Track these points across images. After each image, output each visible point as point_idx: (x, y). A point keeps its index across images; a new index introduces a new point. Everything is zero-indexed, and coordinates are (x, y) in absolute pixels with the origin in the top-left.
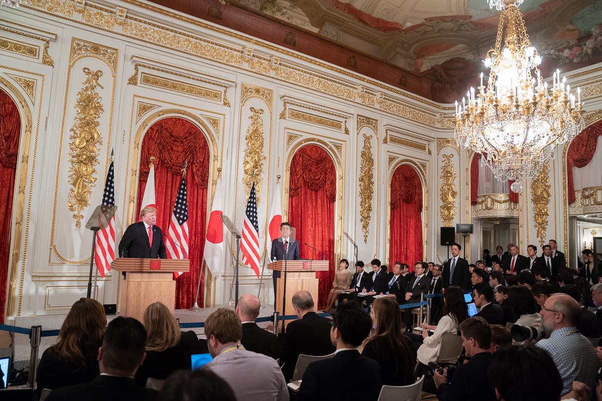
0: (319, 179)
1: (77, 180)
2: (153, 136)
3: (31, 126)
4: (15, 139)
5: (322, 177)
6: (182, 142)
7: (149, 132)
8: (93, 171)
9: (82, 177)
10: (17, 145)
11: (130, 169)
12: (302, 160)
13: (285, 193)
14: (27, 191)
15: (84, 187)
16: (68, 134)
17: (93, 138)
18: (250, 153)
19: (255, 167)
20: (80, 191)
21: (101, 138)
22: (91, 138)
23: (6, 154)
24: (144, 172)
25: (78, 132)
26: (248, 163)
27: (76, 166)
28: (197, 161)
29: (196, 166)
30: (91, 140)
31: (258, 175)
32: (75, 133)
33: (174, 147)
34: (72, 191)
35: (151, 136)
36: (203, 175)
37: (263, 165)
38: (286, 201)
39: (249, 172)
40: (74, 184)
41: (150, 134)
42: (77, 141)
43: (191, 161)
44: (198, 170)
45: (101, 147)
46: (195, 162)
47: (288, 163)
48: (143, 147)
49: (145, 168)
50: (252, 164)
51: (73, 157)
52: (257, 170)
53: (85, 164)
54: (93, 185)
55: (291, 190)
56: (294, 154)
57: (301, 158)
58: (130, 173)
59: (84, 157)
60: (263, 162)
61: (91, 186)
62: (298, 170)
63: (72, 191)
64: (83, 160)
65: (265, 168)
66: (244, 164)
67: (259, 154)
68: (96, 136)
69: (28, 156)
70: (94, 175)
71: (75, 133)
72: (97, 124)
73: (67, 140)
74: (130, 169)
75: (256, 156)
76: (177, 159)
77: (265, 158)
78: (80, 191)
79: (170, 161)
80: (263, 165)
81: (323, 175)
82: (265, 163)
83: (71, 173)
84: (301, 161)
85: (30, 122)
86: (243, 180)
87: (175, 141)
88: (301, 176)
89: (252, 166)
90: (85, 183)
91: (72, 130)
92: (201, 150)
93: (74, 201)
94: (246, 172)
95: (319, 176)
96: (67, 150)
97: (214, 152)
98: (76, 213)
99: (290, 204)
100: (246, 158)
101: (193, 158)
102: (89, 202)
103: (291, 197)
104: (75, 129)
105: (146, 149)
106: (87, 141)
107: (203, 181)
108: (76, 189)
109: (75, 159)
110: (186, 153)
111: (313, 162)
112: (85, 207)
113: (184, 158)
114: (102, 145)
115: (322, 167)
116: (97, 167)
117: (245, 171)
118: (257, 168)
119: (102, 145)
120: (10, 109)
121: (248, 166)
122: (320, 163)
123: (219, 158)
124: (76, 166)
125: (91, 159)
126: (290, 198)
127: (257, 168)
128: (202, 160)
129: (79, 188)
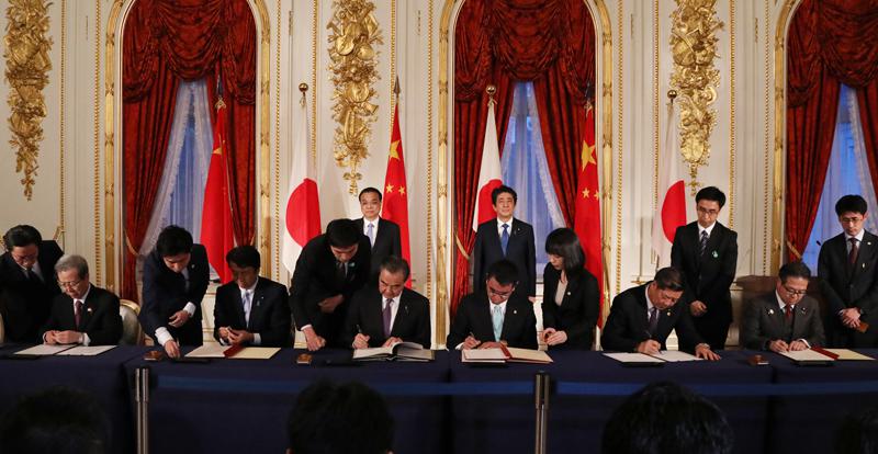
0: (863, 58)
1: (345, 113)
2: (476, 13)
3: (269, 30)
4: (249, 58)
5: (873, 53)
6: (533, 15)
7: (468, 5)
8: (371, 94)
9: (353, 107)
10: (253, 67)
11: (435, 82)
12: (819, 18)
13: (777, 98)
14: (273, 140)
15: (358, 122)
16: (326, 33)
17: (365, 34)
18: (685, 19)
19: (699, 47)
20: (352, 132)
21: (380, 32)
22: (362, 35)
23: (238, 82)
24: (464, 84)
25: (340, 27)
26: (680, 40)
27: (343, 88)
28: (567, 49)
29: (566, 62)
30: (363, 38)
31: (706, 64)
32: (336, 29)
33: (520, 30)
34: (340, 133)
35: (472, 13)
36: (583, 77)
37: (717, 40)
38: (778, 117)
39: (686, 60)
40: (342, 121)
41: (469, 10)
42: (340, 42)
43: (556, 51)
44: (571, 68)
45: (381, 48)
46: (564, 52)
47: (779, 29)
48: (457, 36)
49: (465, 76)
50: (690, 42)
51: (336, 72)
52: (703, 53)
53: (357, 82)
54: (372, 117)
55: (793, 91)
56: (795, 6)
57: (814, 15)
58: (436, 89)
59: (353, 70)
60: (718, 33)
61: (370, 121)
62: (807, 43)
63: (340, 132)
64: (351, 75)
65: (722, 49)
66: (672, 43)
67: (706, 18)
68: (369, 27)
69: (268, 82)
70: (373, 100)
71: (336, 29)
72: (371, 7)
73: (325, 45)
74: (435, 82)
75: (699, 23)
76: (526, 51)
77: (721, 25)
78: (352, 132)
79: (510, 56)
80: (717, 40)
81: (875, 49)
82: (722, 36)
83: (334, 103)
84: (814, 22)
85: (266, 24)
86: (672, 78)
87: (520, 15)
88: (815, 57)
89: (690, 45)
90: (359, 117)
91: (330, 25)
92: (575, 27)
93: (344, 149)
94: (678, 61)
95: (865, 51)
96: (325, 61)
97: (603, 26)
98: (348, 170)
99: (793, 123)
100: (677, 30)
101: (560, 45)
102: (369, 151)
103: (791, 106)
104: (335, 23)
105: (464, 39)
106: (356, 41)
107: (583, 88)
108: (345, 129)
109: (339, 76)
110: (545, 37)
111: (847, 20)
112: (362, 160)
113: (539, 48)
114: (382, 43)
115: (872, 29)
116: (375, 83)
117: (675, 57)
118: (703, 48)
119: (382, 43)
120: (240, 10)
121: (682, 48)
122: (867, 22)
123: (615, 38)
124: (343, 88)
125: (366, 72)
126: (792, 110)
127: (703, 48)
128: (577, 46)
129: (349, 126)
